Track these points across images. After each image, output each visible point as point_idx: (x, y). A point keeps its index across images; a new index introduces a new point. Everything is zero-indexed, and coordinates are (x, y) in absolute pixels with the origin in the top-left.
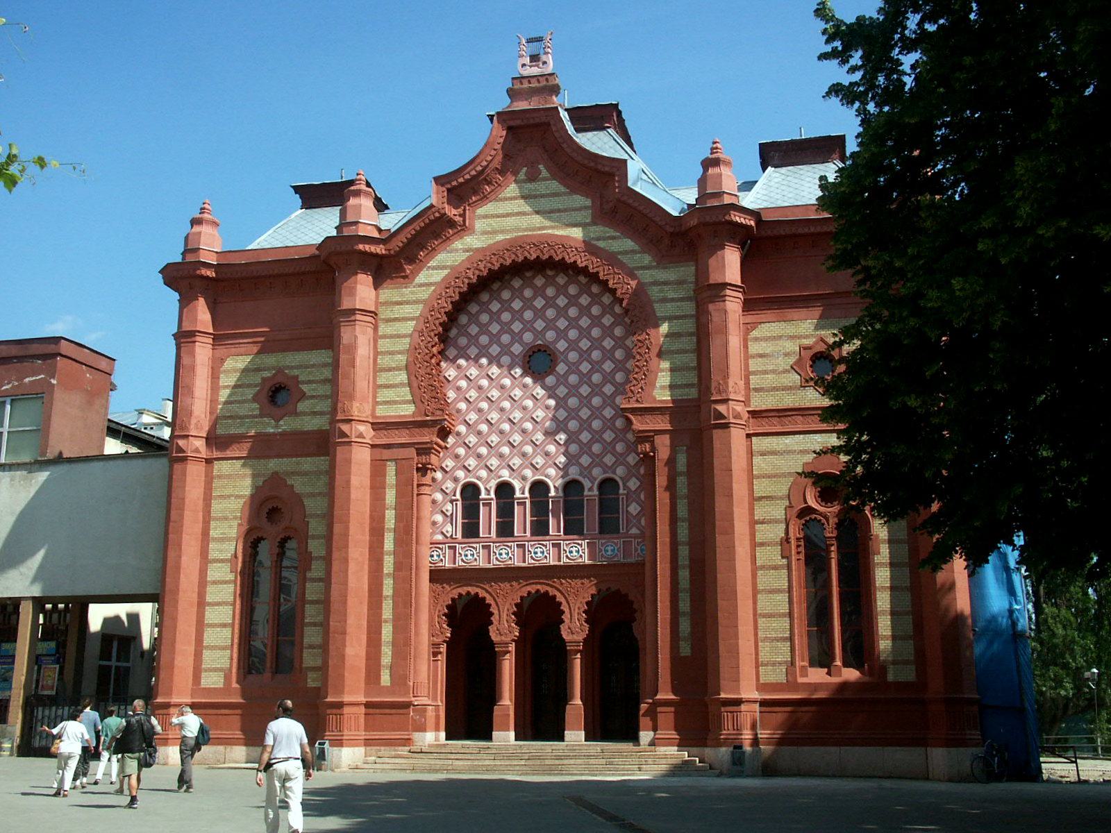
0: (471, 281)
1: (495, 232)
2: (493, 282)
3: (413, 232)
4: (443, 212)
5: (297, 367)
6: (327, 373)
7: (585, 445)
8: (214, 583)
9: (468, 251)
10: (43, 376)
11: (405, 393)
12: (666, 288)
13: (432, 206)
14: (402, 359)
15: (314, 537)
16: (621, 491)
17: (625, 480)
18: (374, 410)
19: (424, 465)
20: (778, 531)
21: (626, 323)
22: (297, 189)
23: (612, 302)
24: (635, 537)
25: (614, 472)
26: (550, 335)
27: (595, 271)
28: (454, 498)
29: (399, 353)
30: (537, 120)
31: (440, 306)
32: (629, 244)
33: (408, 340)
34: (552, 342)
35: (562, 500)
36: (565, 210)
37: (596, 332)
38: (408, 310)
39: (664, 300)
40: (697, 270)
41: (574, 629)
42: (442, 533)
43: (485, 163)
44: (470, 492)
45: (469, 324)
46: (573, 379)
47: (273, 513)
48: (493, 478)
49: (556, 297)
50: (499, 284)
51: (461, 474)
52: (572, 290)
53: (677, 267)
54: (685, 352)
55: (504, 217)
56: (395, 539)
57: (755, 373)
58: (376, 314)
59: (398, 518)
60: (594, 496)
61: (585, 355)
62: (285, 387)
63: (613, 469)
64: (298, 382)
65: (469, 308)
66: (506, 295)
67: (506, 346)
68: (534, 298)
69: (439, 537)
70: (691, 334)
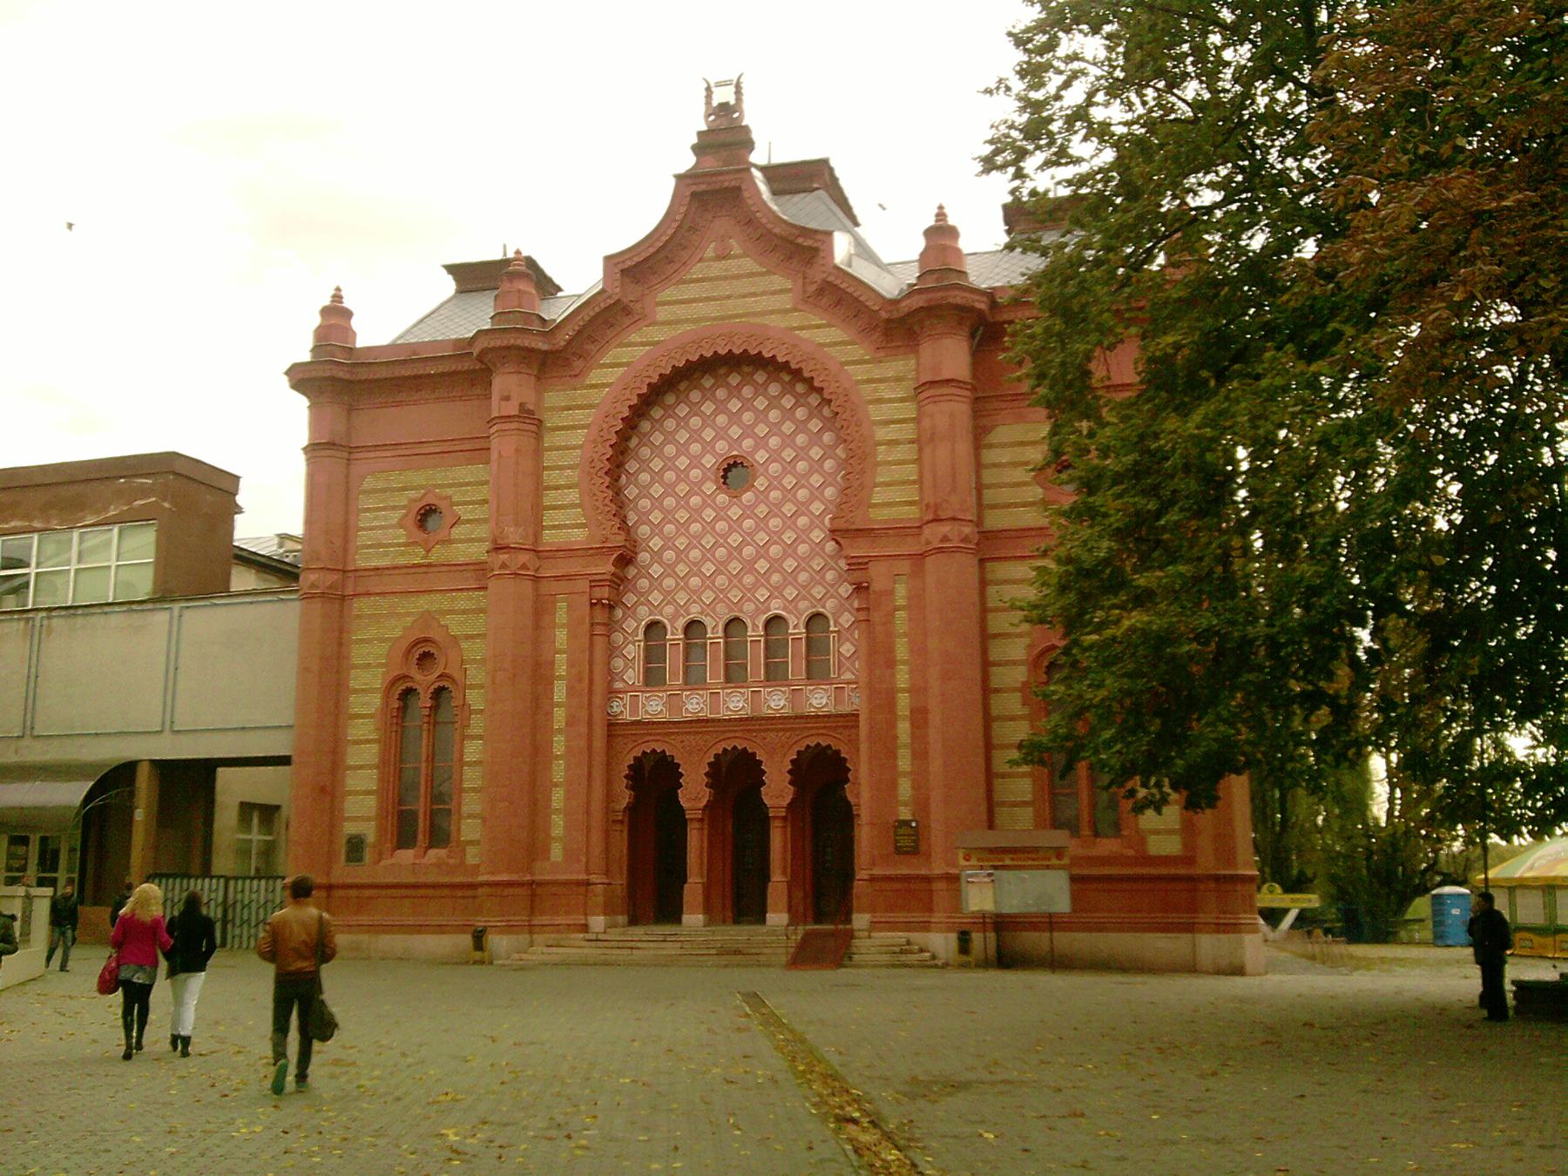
1: (678, 322)
3: (581, 323)
5: (450, 486)
6: (484, 493)
8: (358, 742)
12: (882, 386)
13: (602, 291)
14: (572, 475)
15: (472, 687)
18: (537, 536)
19: (599, 600)
20: (1019, 675)
22: (452, 269)
26: (747, 443)
30: (726, 184)
32: (835, 334)
34: (748, 453)
37: (801, 439)
38: (580, 416)
39: (880, 401)
40: (918, 364)
41: (777, 791)
43: (665, 238)
44: (654, 628)
47: (426, 658)
52: (774, 389)
57: (989, 487)
64: (453, 504)
65: (652, 413)
66: (695, 396)
67: (695, 457)
69: (618, 685)
70: (912, 442)
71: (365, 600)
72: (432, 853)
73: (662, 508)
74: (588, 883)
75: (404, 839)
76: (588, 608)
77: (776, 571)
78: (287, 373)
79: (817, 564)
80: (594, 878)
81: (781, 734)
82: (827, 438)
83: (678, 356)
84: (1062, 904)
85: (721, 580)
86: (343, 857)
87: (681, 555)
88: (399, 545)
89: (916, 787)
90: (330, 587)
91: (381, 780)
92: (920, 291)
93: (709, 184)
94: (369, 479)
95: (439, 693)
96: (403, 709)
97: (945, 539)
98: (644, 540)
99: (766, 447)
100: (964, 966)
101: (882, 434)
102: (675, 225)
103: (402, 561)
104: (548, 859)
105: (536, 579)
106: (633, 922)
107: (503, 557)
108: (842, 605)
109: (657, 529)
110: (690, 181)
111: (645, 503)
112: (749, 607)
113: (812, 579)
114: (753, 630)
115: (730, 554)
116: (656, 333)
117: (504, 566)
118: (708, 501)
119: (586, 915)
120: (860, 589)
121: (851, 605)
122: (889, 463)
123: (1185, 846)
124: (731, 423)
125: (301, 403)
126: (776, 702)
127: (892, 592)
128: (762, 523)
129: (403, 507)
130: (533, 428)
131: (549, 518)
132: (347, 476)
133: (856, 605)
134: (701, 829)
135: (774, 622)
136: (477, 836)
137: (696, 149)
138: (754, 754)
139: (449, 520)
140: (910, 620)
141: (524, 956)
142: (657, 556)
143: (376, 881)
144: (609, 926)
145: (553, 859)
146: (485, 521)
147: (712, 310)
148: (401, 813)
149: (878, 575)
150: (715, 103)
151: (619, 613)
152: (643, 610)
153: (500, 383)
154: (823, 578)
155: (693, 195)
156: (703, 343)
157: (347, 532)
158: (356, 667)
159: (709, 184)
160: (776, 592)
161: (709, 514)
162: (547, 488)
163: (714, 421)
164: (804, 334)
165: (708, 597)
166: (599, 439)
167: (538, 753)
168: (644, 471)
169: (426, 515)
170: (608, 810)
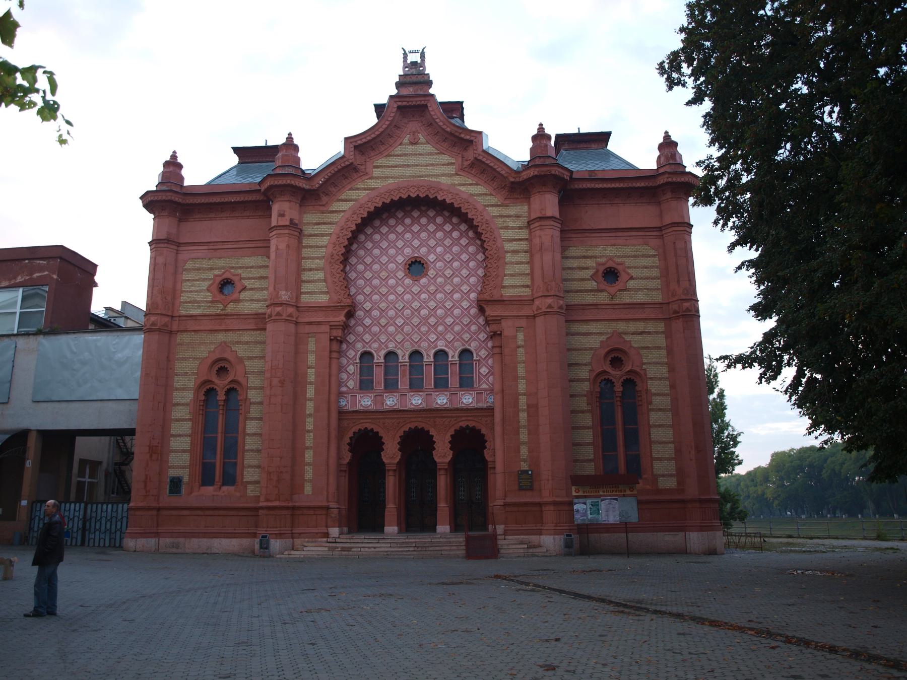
0: (370, 210)
1: (387, 178)
3: (329, 174)
4: (351, 161)
5: (241, 268)
6: (262, 272)
8: (177, 420)
9: (368, 190)
11: (322, 286)
13: (343, 157)
14: (320, 263)
16: (475, 358)
17: (478, 349)
18: (298, 298)
19: (335, 337)
20: (585, 387)
21: (476, 243)
24: (485, 390)
26: (424, 250)
27: (458, 206)
28: (355, 361)
29: (318, 258)
30: (418, 103)
31: (348, 226)
33: (324, 249)
34: (425, 255)
35: (433, 364)
36: (437, 165)
39: (507, 228)
40: (529, 208)
42: (347, 386)
43: (381, 130)
47: (222, 371)
49: (428, 224)
50: (387, 214)
52: (439, 220)
54: (521, 263)
55: (393, 167)
58: (301, 230)
64: (241, 279)
65: (366, 230)
66: (392, 222)
67: (392, 257)
68: (412, 224)
69: (344, 389)
70: (526, 252)
71: (185, 335)
72: (225, 488)
73: (371, 286)
74: (328, 508)
75: (207, 477)
76: (328, 342)
77: (441, 324)
78: (141, 198)
79: (466, 320)
80: (332, 505)
81: (444, 420)
82: (471, 249)
83: (386, 197)
84: (634, 517)
85: (407, 329)
86: (168, 491)
89: (530, 451)
90: (163, 326)
92: (535, 166)
93: (408, 102)
94: (190, 262)
95: (230, 391)
96: (206, 401)
97: (550, 306)
98: (360, 304)
99: (435, 252)
100: (569, 554)
101: (508, 246)
102: (387, 123)
103: (208, 312)
104: (303, 493)
105: (297, 323)
106: (349, 532)
107: (279, 309)
108: (480, 345)
110: (397, 100)
112: (424, 344)
113: (463, 329)
114: (427, 358)
115: (413, 314)
116: (372, 184)
117: (278, 314)
119: (327, 527)
120: (494, 335)
121: (486, 345)
122: (512, 263)
123: (679, 483)
124: (413, 238)
126: (441, 400)
127: (515, 337)
129: (210, 279)
130: (297, 234)
131: (305, 288)
132: (176, 260)
133: (490, 344)
134: (395, 476)
135: (441, 354)
136: (256, 478)
137: (398, 85)
139: (239, 288)
140: (525, 353)
141: (293, 552)
142: (368, 312)
143: (189, 505)
144: (341, 533)
145: (306, 493)
146: (262, 289)
147: (408, 172)
149: (507, 327)
150: (409, 62)
151: (344, 346)
152: (359, 345)
153: (276, 208)
154: (469, 329)
155: (399, 108)
156: (401, 191)
158: (177, 375)
160: (441, 336)
162: (304, 270)
164: (463, 188)
165: (399, 338)
166: (337, 243)
168: (361, 263)
169: (225, 284)
170: (339, 465)
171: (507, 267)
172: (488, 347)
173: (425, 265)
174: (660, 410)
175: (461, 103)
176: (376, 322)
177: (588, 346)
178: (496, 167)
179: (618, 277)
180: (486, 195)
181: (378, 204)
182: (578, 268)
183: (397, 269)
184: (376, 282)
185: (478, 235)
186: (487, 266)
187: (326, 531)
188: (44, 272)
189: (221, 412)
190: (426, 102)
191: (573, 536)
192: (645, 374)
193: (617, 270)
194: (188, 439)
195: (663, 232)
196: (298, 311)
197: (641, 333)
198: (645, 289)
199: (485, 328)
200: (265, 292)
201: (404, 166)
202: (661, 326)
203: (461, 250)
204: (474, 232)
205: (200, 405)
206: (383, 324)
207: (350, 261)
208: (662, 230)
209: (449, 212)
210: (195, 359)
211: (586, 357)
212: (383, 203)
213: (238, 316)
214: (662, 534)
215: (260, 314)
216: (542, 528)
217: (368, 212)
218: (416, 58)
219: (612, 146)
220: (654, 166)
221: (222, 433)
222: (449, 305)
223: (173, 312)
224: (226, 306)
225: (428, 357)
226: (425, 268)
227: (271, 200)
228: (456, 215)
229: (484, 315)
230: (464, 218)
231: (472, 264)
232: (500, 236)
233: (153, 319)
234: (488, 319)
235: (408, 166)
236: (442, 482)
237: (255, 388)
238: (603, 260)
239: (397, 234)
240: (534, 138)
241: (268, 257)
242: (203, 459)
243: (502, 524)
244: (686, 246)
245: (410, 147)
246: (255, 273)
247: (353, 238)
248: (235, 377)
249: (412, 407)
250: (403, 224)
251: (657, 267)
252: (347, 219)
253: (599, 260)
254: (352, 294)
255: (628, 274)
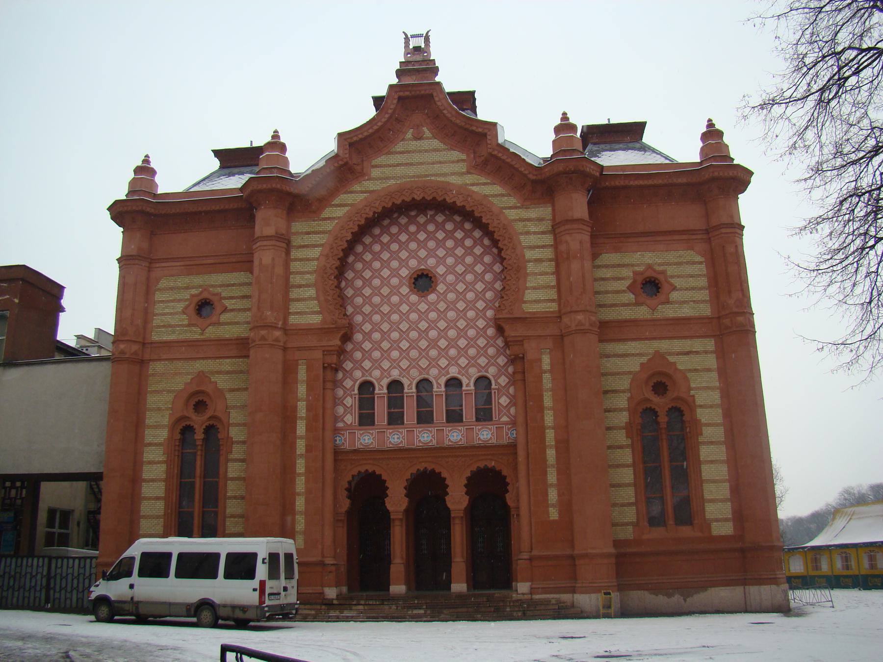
1: (388, 178)
2: (384, 220)
4: (345, 160)
5: (221, 286)
6: (245, 290)
7: (462, 349)
8: (149, 463)
10: (8, 297)
11: (314, 305)
12: (529, 224)
14: (311, 278)
16: (493, 386)
17: (497, 377)
19: (330, 365)
20: (623, 418)
21: (493, 253)
23: (482, 235)
24: (506, 423)
25: (487, 371)
26: (432, 262)
28: (353, 393)
29: (308, 273)
30: (423, 92)
32: (497, 189)
33: (315, 263)
34: (432, 267)
35: (444, 394)
39: (528, 233)
40: (554, 210)
44: (366, 387)
45: (363, 253)
46: (451, 296)
47: (200, 406)
48: (386, 377)
49: (436, 231)
51: (358, 374)
52: (449, 226)
53: (538, 207)
54: (546, 274)
55: (395, 166)
56: (307, 425)
59: (309, 408)
60: (470, 390)
61: (460, 277)
62: (209, 302)
63: (486, 368)
66: (394, 230)
68: (418, 232)
69: (340, 425)
70: (550, 260)
73: (371, 305)
76: (322, 370)
79: (482, 342)
82: (487, 259)
85: (414, 353)
87: (385, 335)
88: (182, 325)
89: (560, 495)
91: (168, 490)
95: (210, 430)
96: (183, 441)
98: (358, 325)
102: (387, 116)
107: (263, 332)
108: (499, 370)
109: (367, 318)
111: (359, 300)
112: (434, 372)
117: (263, 338)
118: (404, 299)
119: (323, 586)
120: (516, 359)
121: (507, 370)
125: (117, 232)
128: (442, 315)
130: (284, 245)
131: (294, 307)
133: (511, 370)
135: (454, 383)
137: (399, 73)
138: (440, 473)
140: (553, 379)
142: (368, 336)
147: (411, 171)
148: (179, 512)
149: (530, 349)
150: (411, 47)
151: (340, 375)
152: (358, 374)
153: (261, 215)
154: (486, 352)
155: (400, 98)
157: (147, 315)
159: (411, 92)
160: (453, 361)
161: (404, 308)
163: (407, 246)
165: (404, 364)
167: (287, 472)
171: (529, 278)
172: (509, 373)
173: (432, 279)
174: (712, 443)
175: (472, 94)
176: (377, 345)
177: (626, 369)
178: (513, 163)
179: (660, 288)
180: (503, 195)
181: (377, 209)
182: (612, 278)
183: (401, 285)
184: (376, 300)
185: (495, 243)
186: (505, 277)
187: (321, 591)
188: (5, 295)
189: (199, 453)
190: (431, 91)
191: (613, 595)
192: (694, 401)
193: (659, 280)
194: (162, 485)
195: (711, 235)
196: (286, 334)
197: (688, 353)
198: (691, 301)
199: (505, 351)
200: (249, 314)
201: (407, 164)
202: (710, 344)
203: (475, 260)
204: (489, 239)
205: (175, 445)
206: (385, 349)
207: (346, 275)
208: (708, 233)
209: (460, 216)
210: (169, 391)
211: (624, 383)
212: (384, 207)
213: (221, 342)
214: (717, 589)
215: (242, 339)
216: (577, 585)
217: (366, 219)
218: (421, 43)
219: (648, 138)
220: (697, 159)
221: (200, 477)
222: (462, 325)
223: (144, 338)
224: (205, 330)
225: (439, 388)
226: (433, 282)
227: (254, 207)
228: (468, 220)
229: (503, 336)
230: (478, 223)
231: (488, 277)
232: (520, 242)
233: (122, 346)
234: (508, 340)
235: (412, 164)
236: (458, 534)
237: (238, 425)
238: (641, 269)
239: (400, 243)
240: (558, 130)
241: (252, 273)
242: (179, 508)
243: (526, 581)
244: (737, 251)
245: (414, 143)
246: (237, 292)
247: (349, 249)
248: (214, 412)
249: (421, 445)
250: (406, 231)
251: (704, 276)
252: (342, 227)
253: (637, 269)
254: (348, 313)
255: (671, 284)
